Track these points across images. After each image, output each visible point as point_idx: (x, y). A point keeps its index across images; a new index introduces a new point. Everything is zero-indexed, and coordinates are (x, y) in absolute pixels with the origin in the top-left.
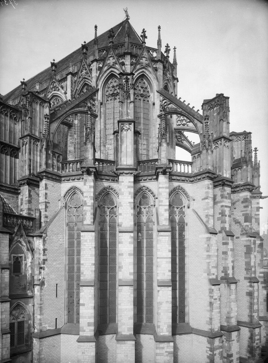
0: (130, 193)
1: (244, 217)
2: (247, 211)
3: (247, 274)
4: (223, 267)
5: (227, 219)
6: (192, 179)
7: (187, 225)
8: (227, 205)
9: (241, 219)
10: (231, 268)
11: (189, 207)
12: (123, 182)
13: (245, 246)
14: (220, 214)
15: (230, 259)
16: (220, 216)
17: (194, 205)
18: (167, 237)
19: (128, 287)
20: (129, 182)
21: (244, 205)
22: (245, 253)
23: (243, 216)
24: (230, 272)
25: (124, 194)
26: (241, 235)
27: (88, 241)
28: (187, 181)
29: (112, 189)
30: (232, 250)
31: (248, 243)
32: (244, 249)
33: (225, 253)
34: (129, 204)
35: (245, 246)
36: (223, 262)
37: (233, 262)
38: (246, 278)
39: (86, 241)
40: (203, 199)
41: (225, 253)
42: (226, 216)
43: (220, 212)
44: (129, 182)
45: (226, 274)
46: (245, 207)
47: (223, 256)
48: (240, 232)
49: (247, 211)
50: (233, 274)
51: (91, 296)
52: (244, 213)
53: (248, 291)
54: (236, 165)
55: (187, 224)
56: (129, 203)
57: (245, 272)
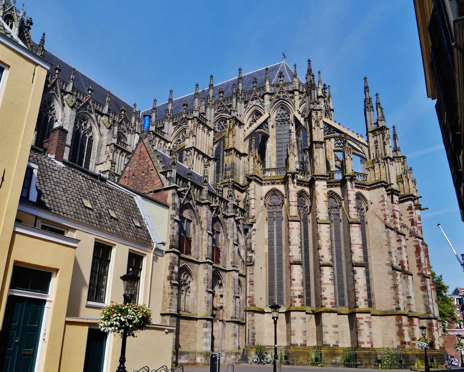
0: (325, 194)
1: (410, 221)
2: (412, 216)
3: (419, 270)
4: (400, 261)
5: (398, 220)
6: (367, 187)
7: (366, 224)
8: (397, 210)
9: (409, 224)
10: (406, 262)
11: (367, 209)
12: (318, 185)
13: (414, 246)
14: (392, 216)
15: (404, 254)
16: (393, 218)
17: (371, 207)
18: (358, 228)
19: (329, 267)
20: (324, 185)
22: (416, 252)
23: (410, 221)
24: (406, 265)
25: (320, 194)
26: (409, 236)
27: (295, 229)
28: (364, 188)
29: (305, 192)
30: (405, 247)
31: (416, 244)
32: (414, 249)
33: (400, 249)
34: (324, 202)
35: (414, 246)
36: (399, 256)
37: (407, 257)
38: (418, 274)
39: (293, 228)
40: (379, 202)
41: (400, 249)
42: (397, 218)
43: (392, 214)
44: (324, 185)
45: (403, 267)
46: (410, 213)
47: (398, 251)
48: (409, 235)
49: (412, 216)
50: (408, 268)
51: (300, 273)
52: (410, 218)
53: (422, 285)
54: (400, 180)
55: (367, 223)
56: (324, 201)
57: (417, 268)
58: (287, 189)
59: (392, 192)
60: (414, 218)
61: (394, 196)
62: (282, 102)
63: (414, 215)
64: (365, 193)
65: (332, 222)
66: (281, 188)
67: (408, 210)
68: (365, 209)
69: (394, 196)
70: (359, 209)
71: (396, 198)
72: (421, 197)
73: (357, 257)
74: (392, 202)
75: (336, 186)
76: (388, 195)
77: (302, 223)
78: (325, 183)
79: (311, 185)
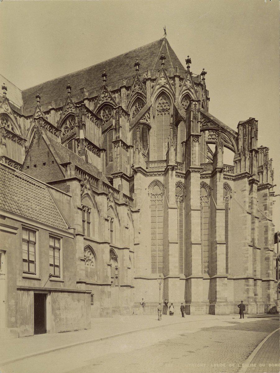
12: (193, 177)
17: (235, 196)
21: (264, 198)
58: (167, 181)
59: (252, 182)
60: (267, 203)
61: (254, 185)
62: (163, 90)
63: (267, 201)
64: (231, 183)
65: (202, 209)
66: (161, 179)
67: (263, 197)
68: (229, 198)
69: (254, 185)
70: (224, 197)
71: (255, 187)
72: (275, 185)
73: (220, 236)
74: (251, 190)
75: (207, 177)
76: (250, 184)
77: (179, 210)
78: (198, 175)
79: (187, 176)
